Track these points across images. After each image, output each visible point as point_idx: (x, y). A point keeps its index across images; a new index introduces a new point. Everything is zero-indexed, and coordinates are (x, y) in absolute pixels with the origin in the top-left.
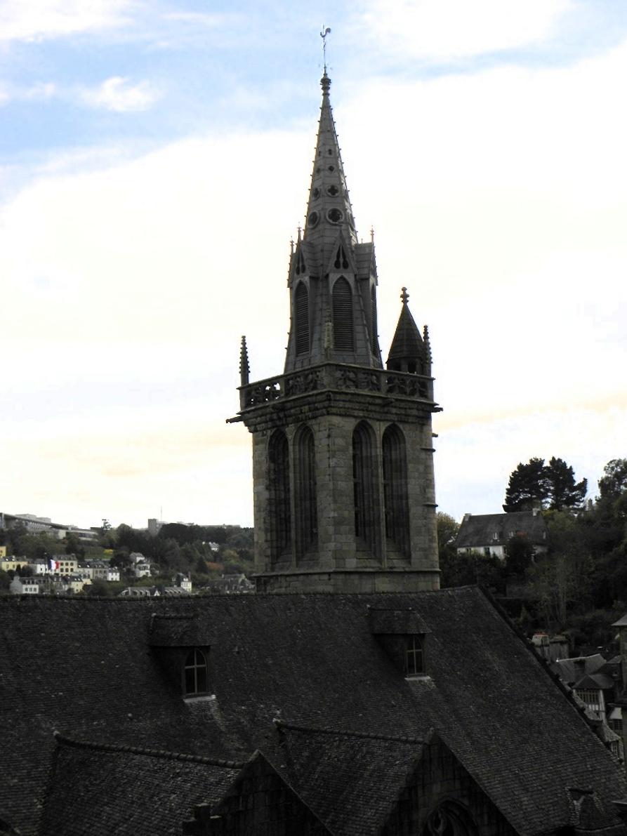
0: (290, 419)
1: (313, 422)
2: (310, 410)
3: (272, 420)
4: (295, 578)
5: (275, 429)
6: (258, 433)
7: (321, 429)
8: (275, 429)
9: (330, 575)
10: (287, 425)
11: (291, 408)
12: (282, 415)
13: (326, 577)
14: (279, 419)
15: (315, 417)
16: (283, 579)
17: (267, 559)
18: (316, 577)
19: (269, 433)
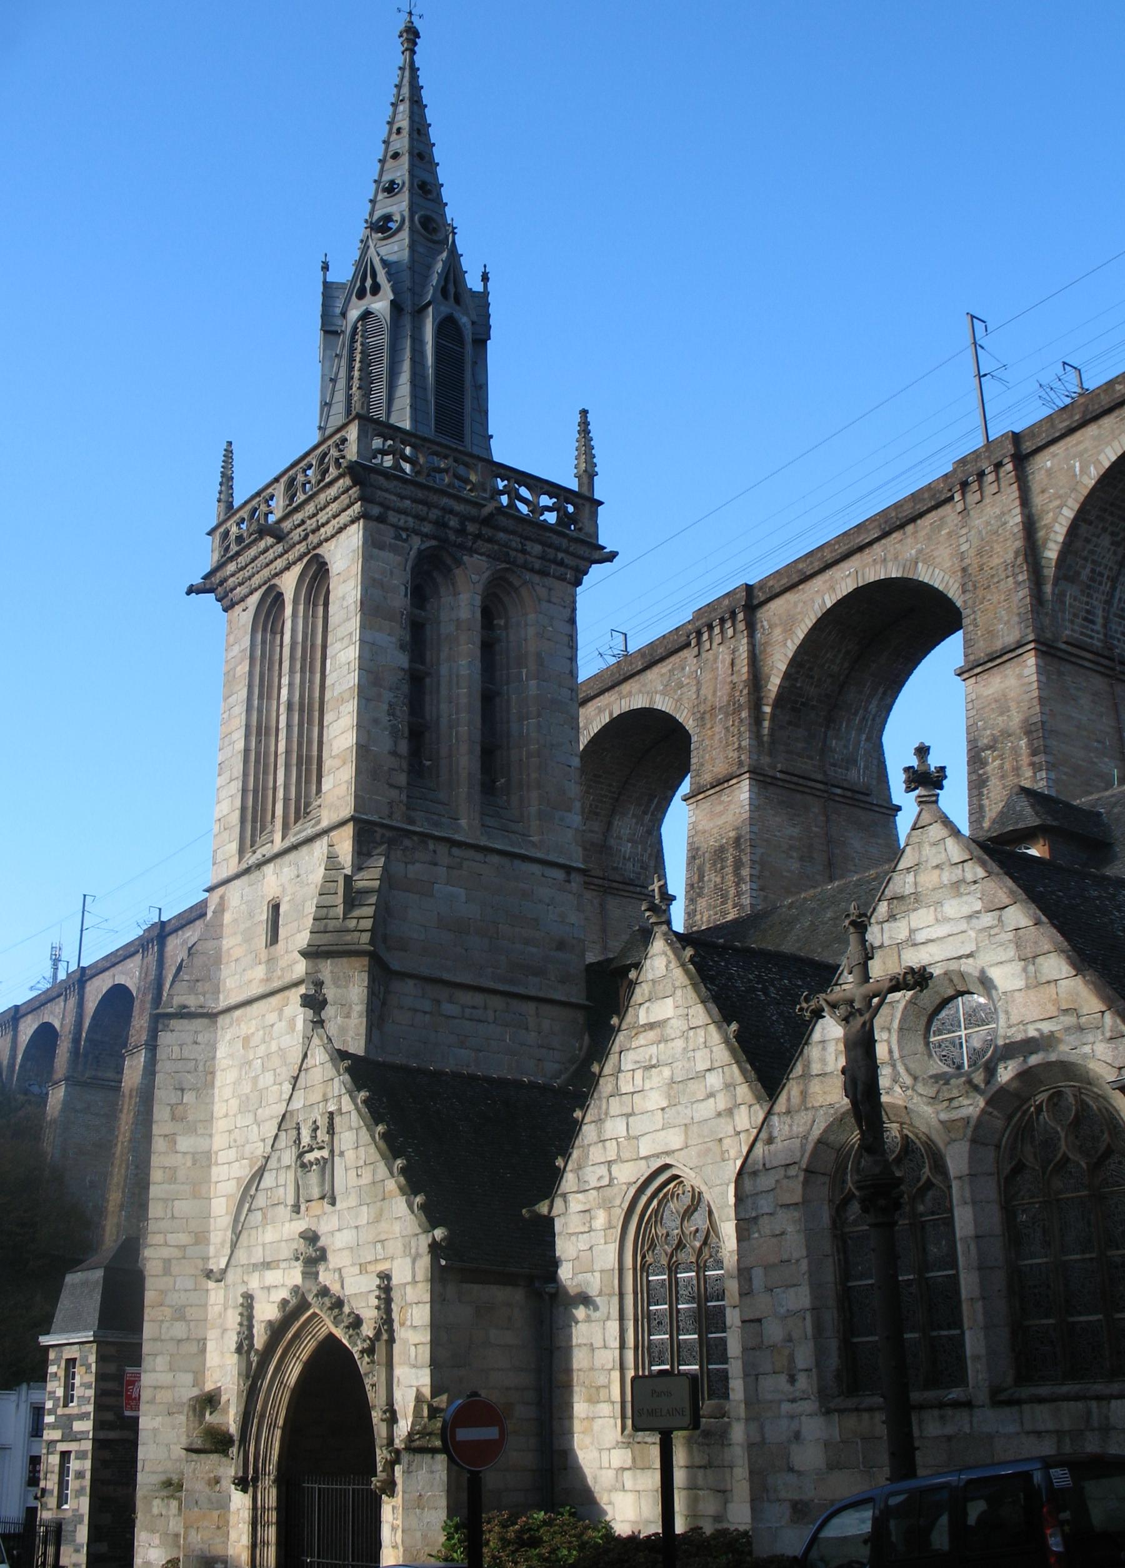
0: (486, 547)
1: (536, 578)
2: (542, 558)
3: (441, 524)
4: (479, 856)
5: (434, 543)
6: (382, 526)
7: (554, 600)
8: (434, 543)
9: (568, 874)
10: (471, 551)
11: (505, 530)
12: (471, 528)
13: (560, 875)
14: (462, 531)
15: (543, 573)
16: (442, 849)
17: (394, 793)
18: (536, 869)
19: (416, 542)
